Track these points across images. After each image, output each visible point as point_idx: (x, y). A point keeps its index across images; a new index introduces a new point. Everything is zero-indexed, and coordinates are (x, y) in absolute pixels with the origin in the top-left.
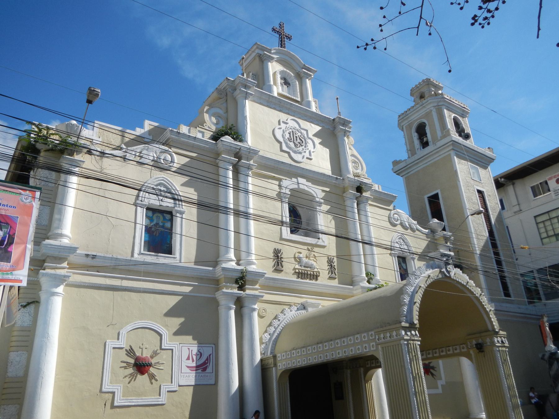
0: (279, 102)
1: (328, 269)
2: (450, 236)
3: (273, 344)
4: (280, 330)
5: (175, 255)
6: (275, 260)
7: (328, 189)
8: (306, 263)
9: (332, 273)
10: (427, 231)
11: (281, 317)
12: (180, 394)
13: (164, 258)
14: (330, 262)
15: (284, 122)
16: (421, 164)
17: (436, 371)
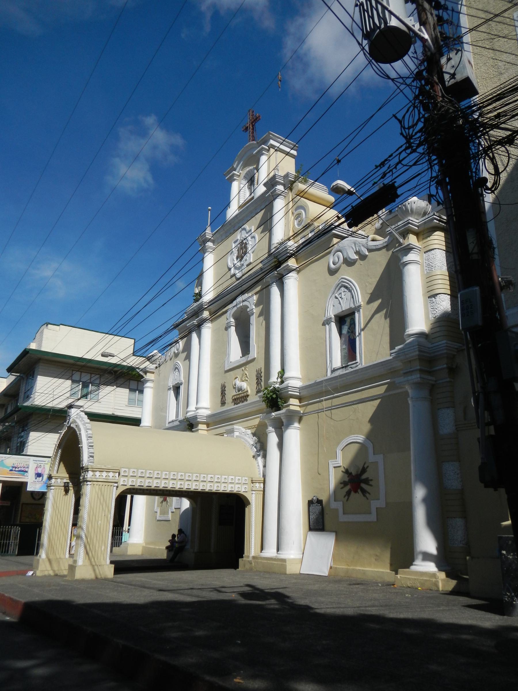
17: (371, 485)
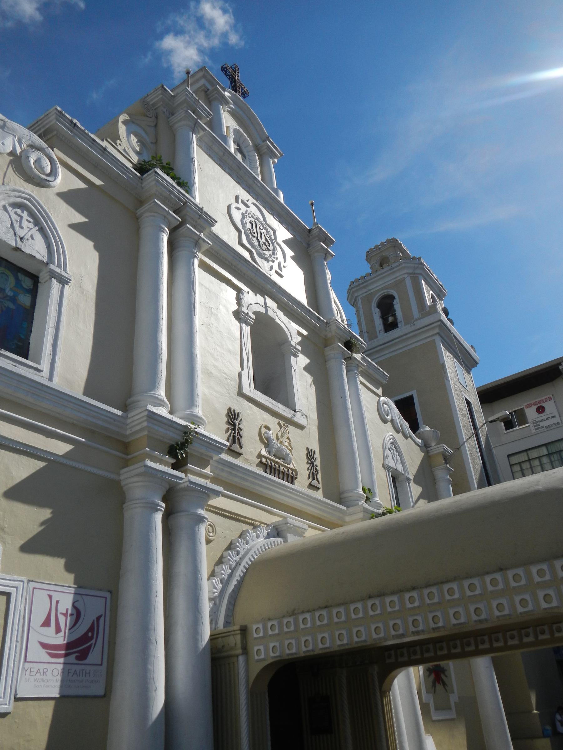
0: (239, 167)
1: (308, 469)
2: (450, 454)
3: (229, 603)
4: (242, 574)
5: (39, 363)
6: (230, 431)
7: (305, 333)
8: (278, 450)
9: (313, 479)
10: (420, 441)
11: (242, 547)
12: (15, 722)
13: (15, 364)
14: (310, 455)
15: (243, 202)
16: (387, 352)
17: (446, 676)
